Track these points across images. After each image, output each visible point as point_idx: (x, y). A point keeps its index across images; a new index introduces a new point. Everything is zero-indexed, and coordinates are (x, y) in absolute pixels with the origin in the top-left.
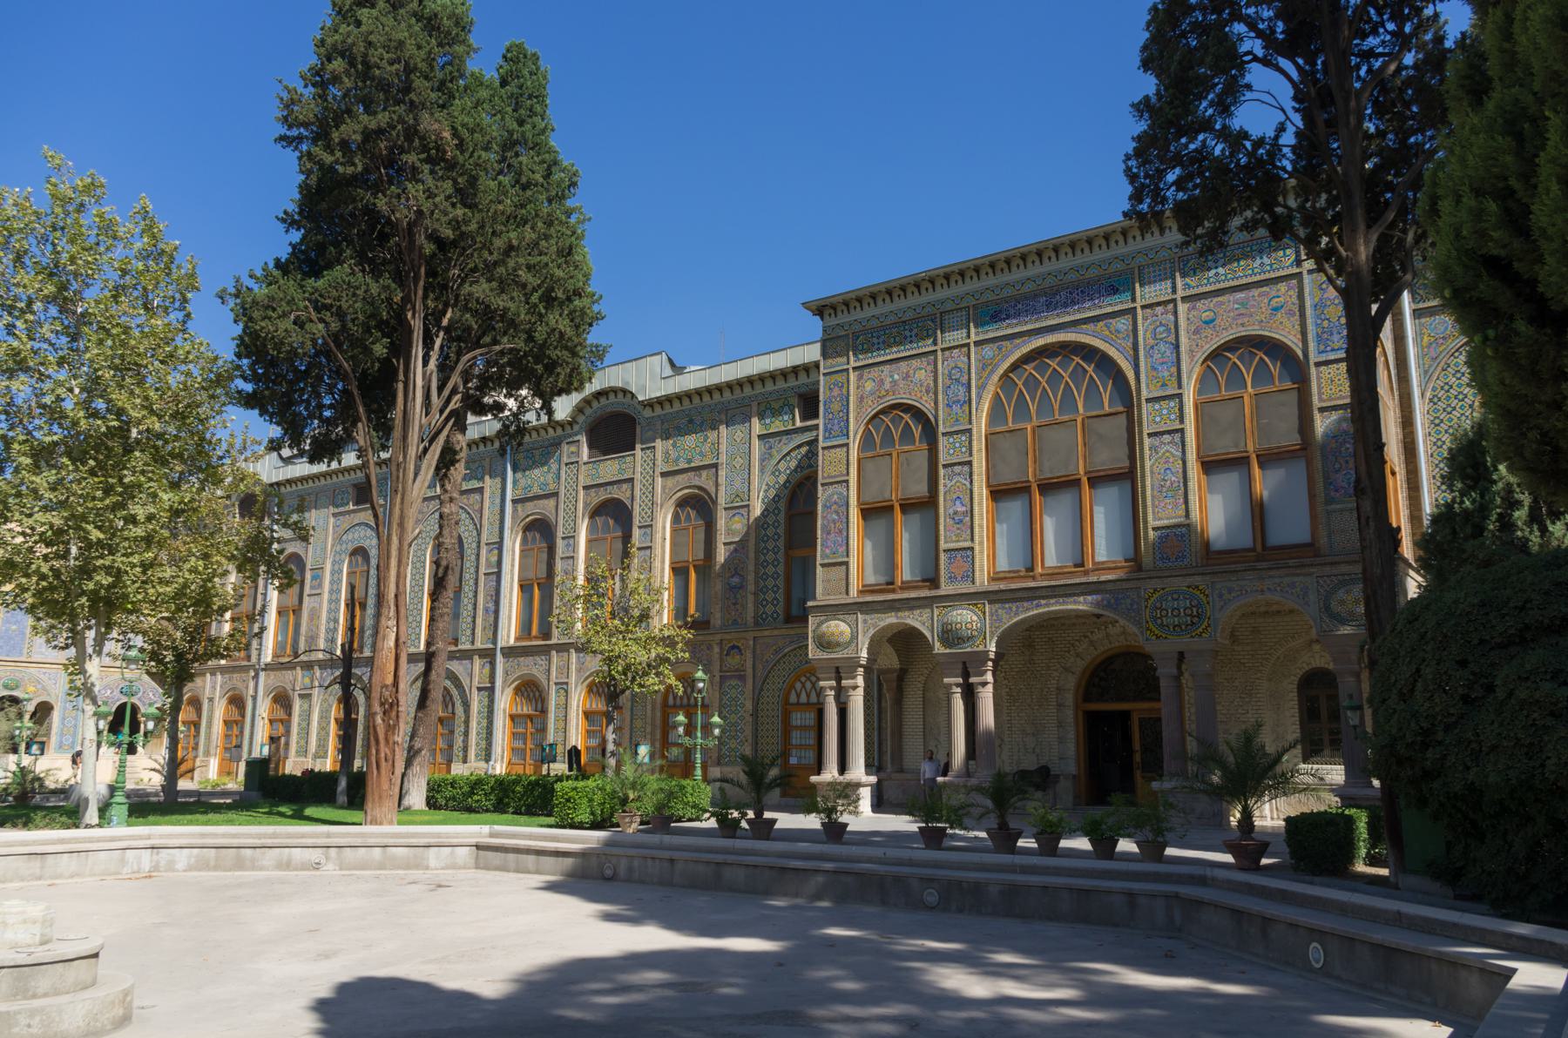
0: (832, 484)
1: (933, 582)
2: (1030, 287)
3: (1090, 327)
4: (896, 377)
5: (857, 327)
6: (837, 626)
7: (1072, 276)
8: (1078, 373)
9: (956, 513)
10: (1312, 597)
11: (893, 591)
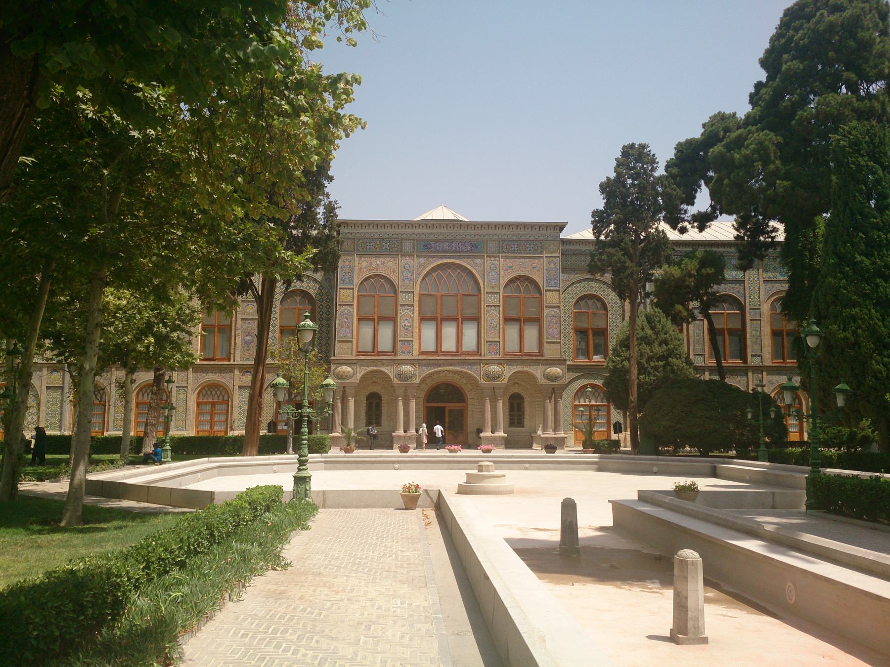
0: (344, 305)
1: (394, 352)
2: (441, 237)
4: (378, 262)
5: (359, 235)
6: (342, 369)
7: (459, 237)
9: (405, 325)
11: (374, 355)
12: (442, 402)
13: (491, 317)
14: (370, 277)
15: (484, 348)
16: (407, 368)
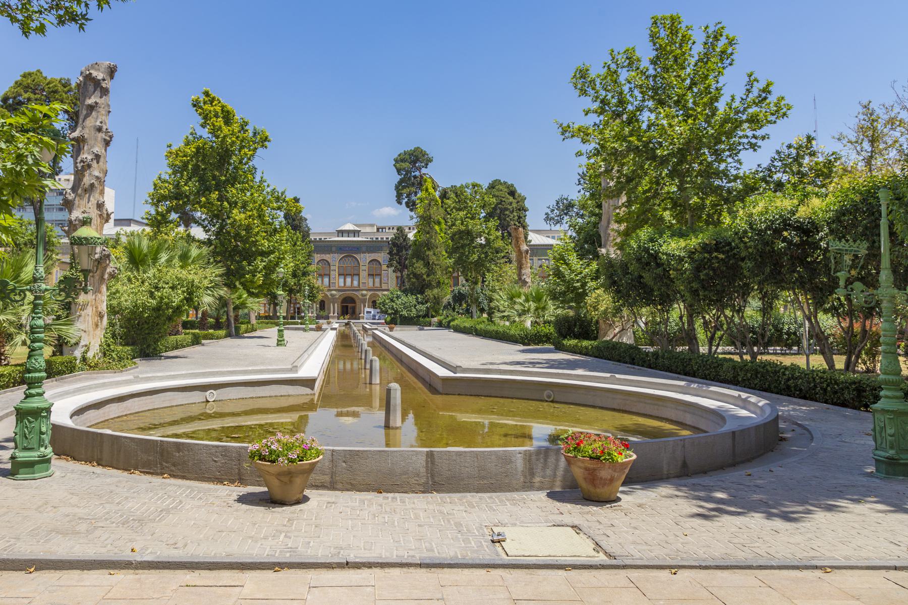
13: (364, 274)
15: (361, 285)
16: (334, 292)
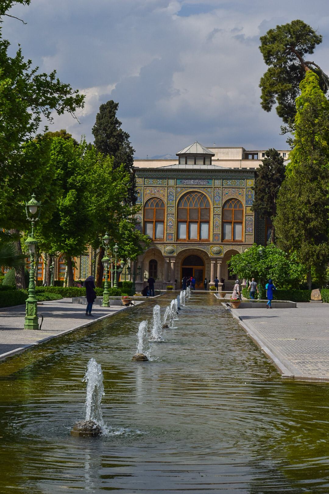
3: (202, 189)
4: (155, 191)
8: (199, 198)
10: (241, 250)
12: (191, 265)
14: (151, 198)
